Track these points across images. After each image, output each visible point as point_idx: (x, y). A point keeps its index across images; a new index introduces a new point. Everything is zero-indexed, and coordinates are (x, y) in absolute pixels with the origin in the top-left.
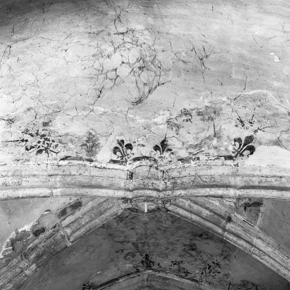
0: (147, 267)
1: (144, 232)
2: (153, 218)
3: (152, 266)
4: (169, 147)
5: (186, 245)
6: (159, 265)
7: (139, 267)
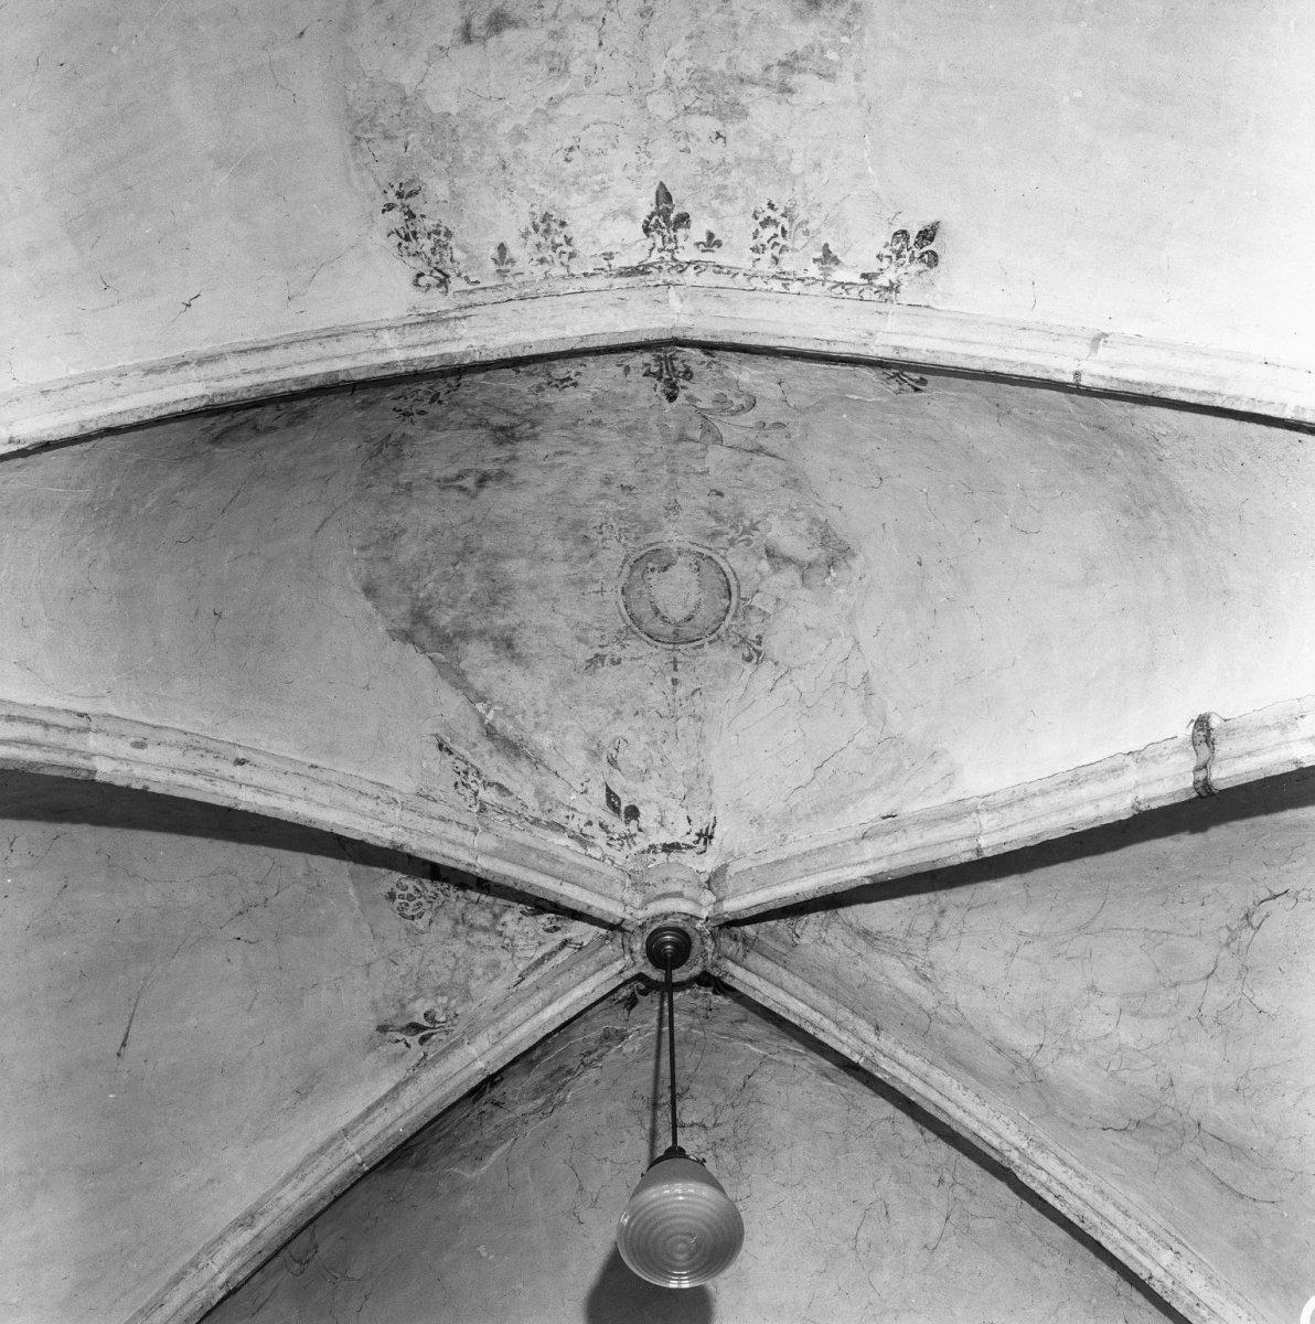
1: (680, 479)
2: (647, 531)
3: (653, 363)
4: (621, 1005)
5: (528, 438)
7: (703, 363)
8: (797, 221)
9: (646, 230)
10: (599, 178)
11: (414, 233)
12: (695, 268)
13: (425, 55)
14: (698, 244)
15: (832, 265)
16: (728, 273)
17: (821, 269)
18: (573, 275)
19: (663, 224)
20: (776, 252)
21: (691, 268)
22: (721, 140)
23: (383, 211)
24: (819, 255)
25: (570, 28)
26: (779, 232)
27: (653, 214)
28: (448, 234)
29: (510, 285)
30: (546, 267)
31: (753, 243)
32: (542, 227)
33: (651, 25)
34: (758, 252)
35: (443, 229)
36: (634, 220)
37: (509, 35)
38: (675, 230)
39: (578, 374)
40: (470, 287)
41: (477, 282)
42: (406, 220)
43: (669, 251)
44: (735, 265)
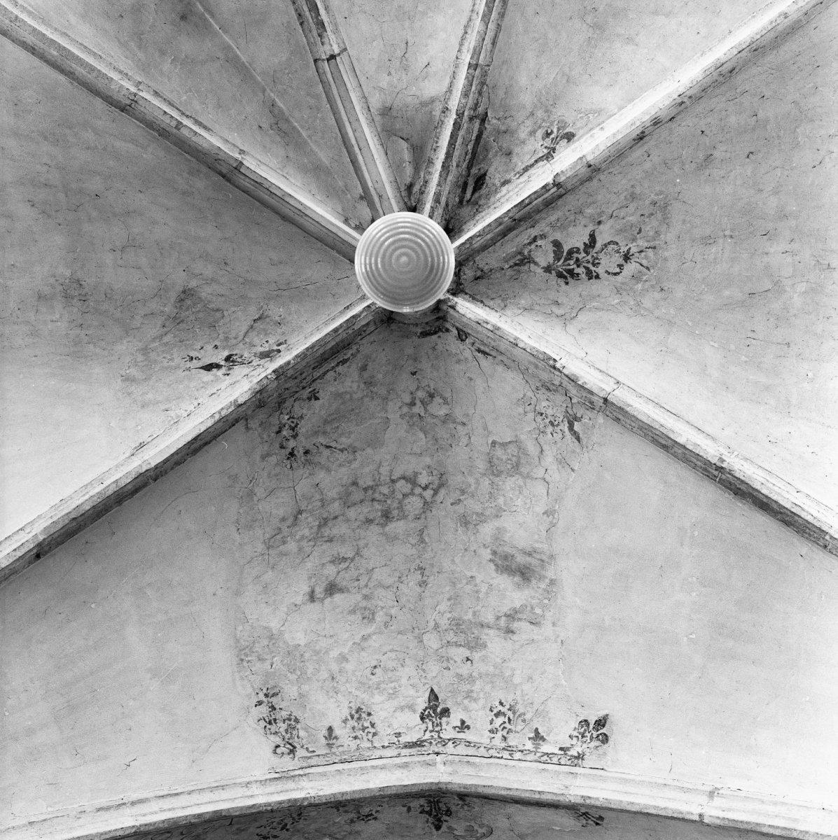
0: (438, 802)
3: (426, 805)
6: (409, 809)
7: (458, 805)
8: (518, 713)
9: (422, 718)
10: (392, 685)
11: (275, 720)
12: (453, 743)
13: (285, 609)
14: (455, 728)
15: (541, 742)
16: (474, 746)
17: (533, 744)
18: (375, 747)
19: (433, 715)
20: (505, 733)
21: (451, 743)
22: (469, 662)
23: (256, 706)
24: (532, 735)
25: (376, 593)
26: (507, 720)
27: (426, 708)
28: (297, 721)
29: (334, 753)
30: (358, 741)
31: (490, 727)
32: (356, 716)
33: (426, 591)
34: (493, 733)
35: (293, 718)
36: (414, 711)
37: (338, 597)
38: (440, 719)
39: (377, 811)
40: (309, 755)
41: (314, 751)
42: (270, 712)
43: (437, 732)
44: (479, 742)
